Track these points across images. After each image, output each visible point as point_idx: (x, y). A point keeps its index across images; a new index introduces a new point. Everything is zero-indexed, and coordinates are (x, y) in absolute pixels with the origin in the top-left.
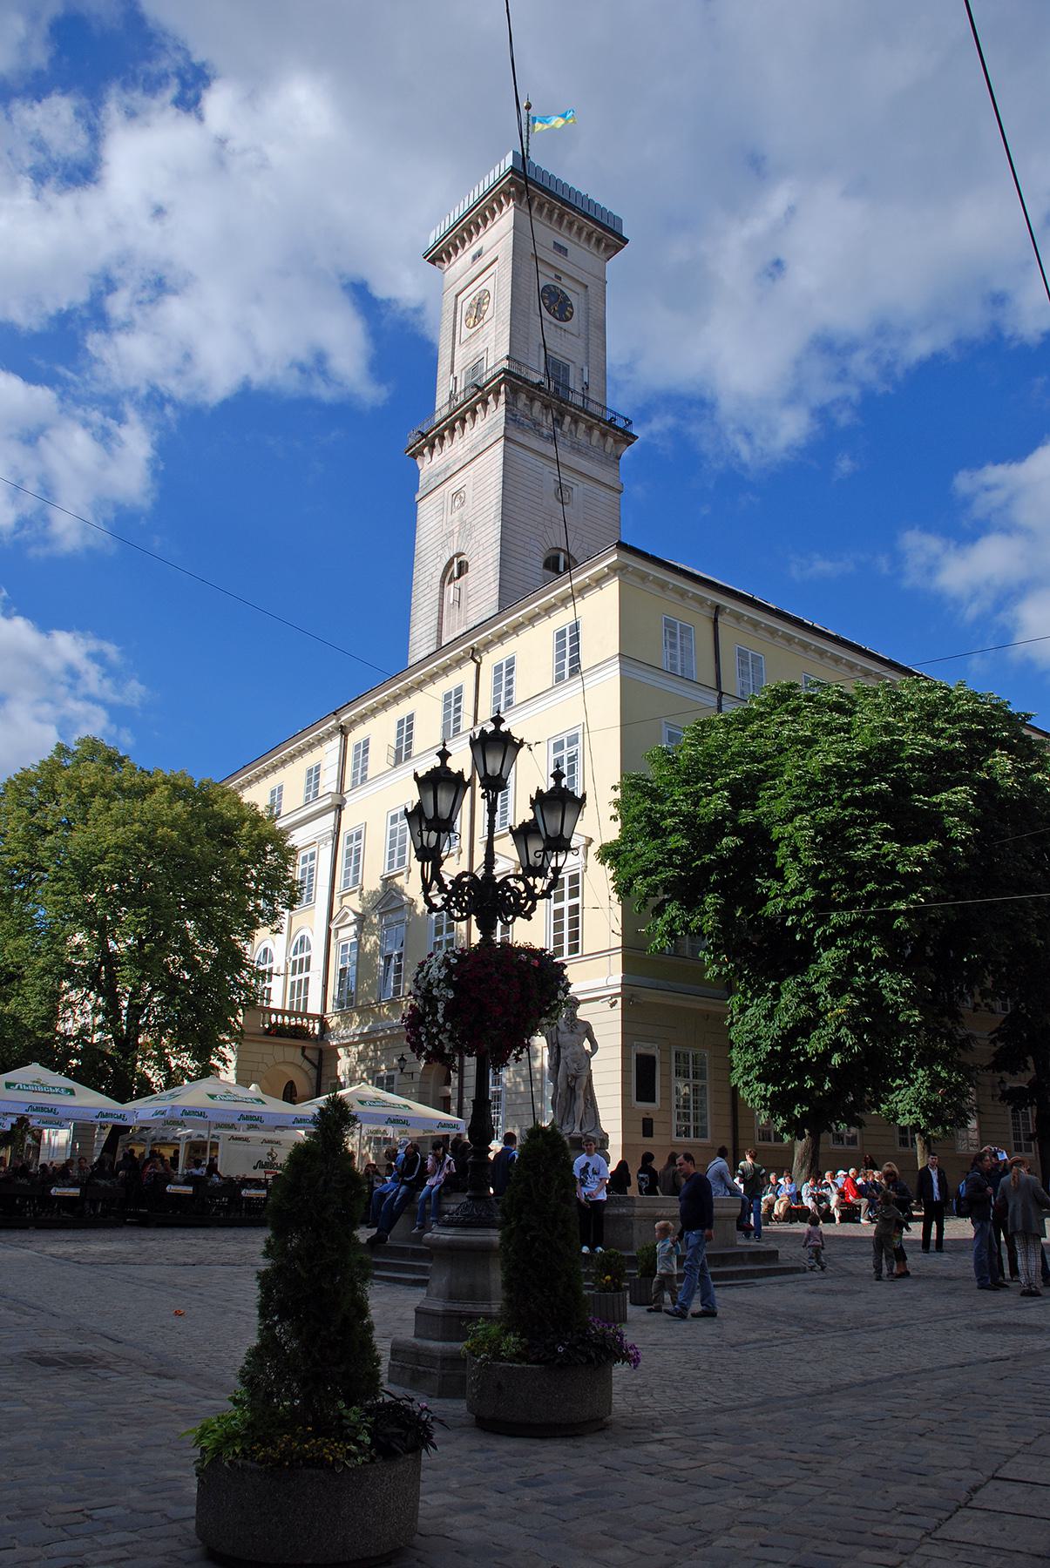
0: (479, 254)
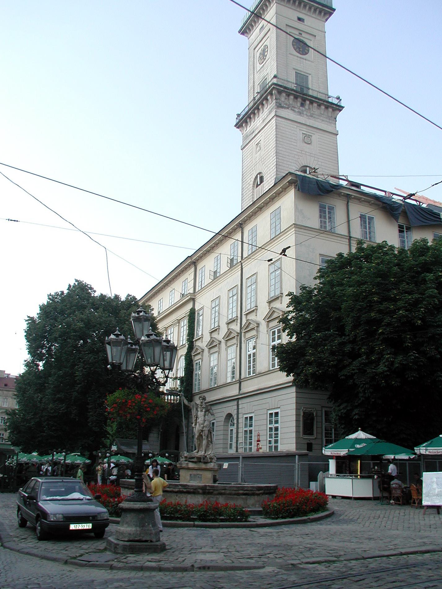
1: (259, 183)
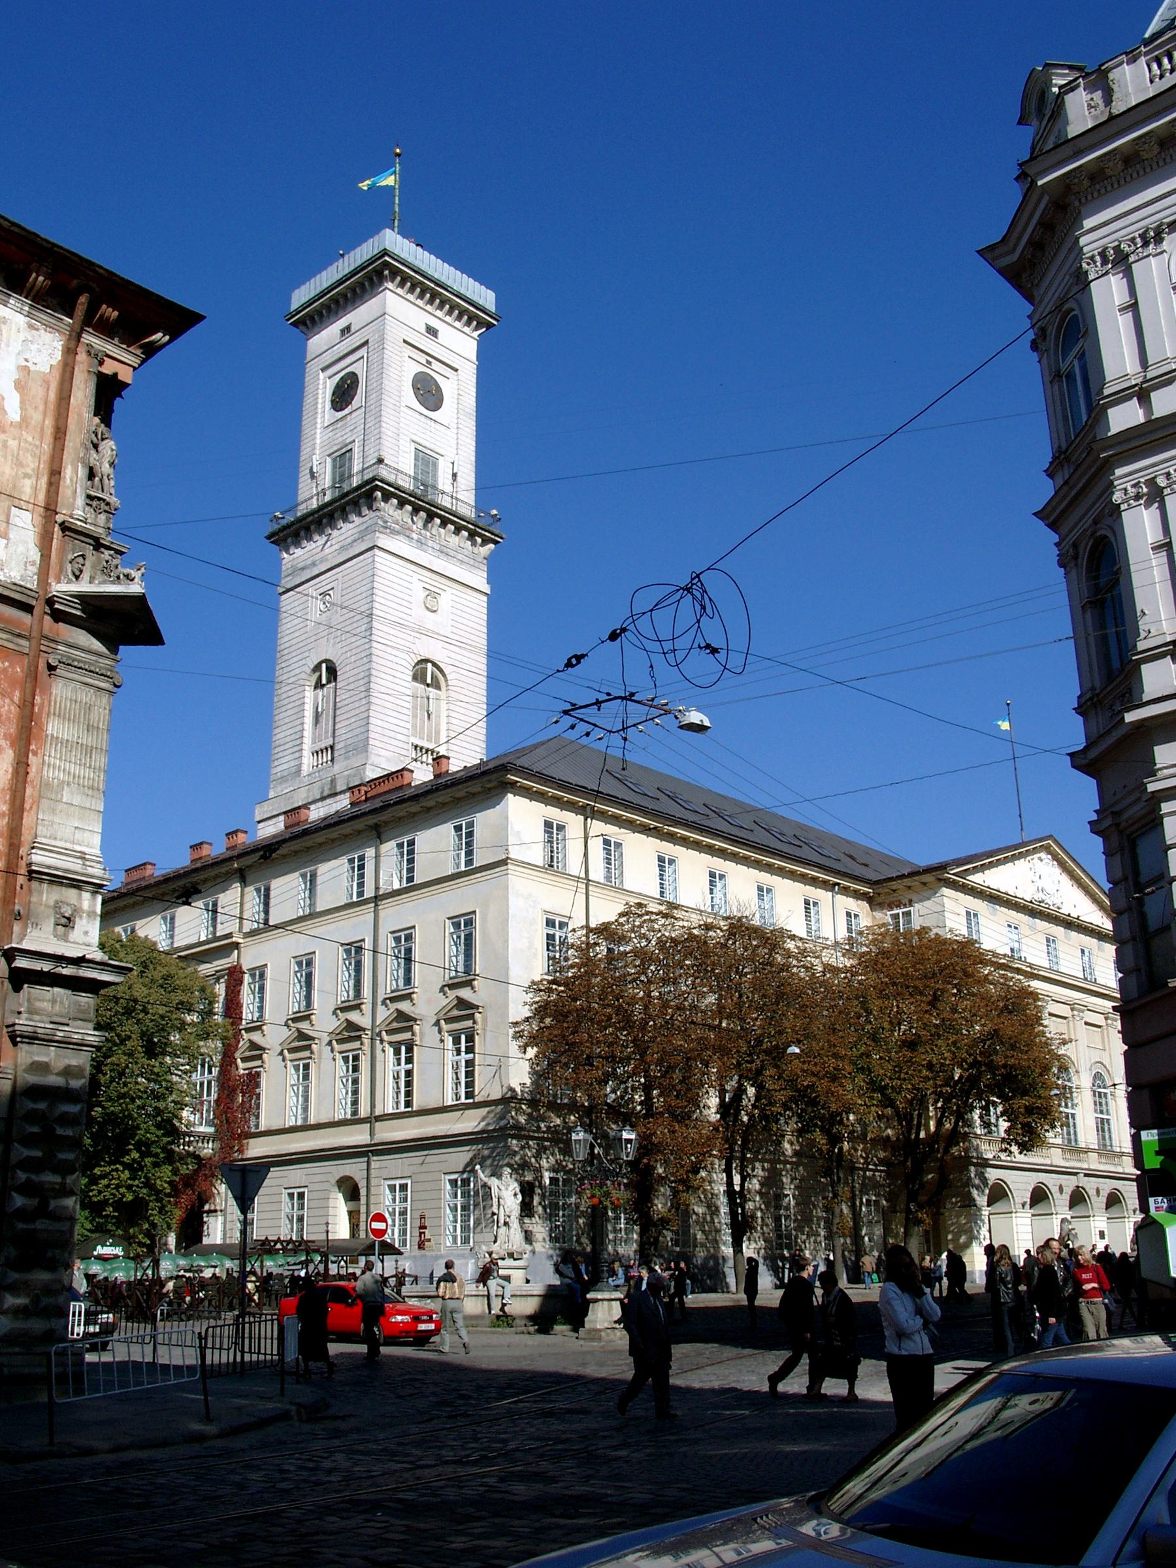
0: (346, 331)
1: (324, 681)
